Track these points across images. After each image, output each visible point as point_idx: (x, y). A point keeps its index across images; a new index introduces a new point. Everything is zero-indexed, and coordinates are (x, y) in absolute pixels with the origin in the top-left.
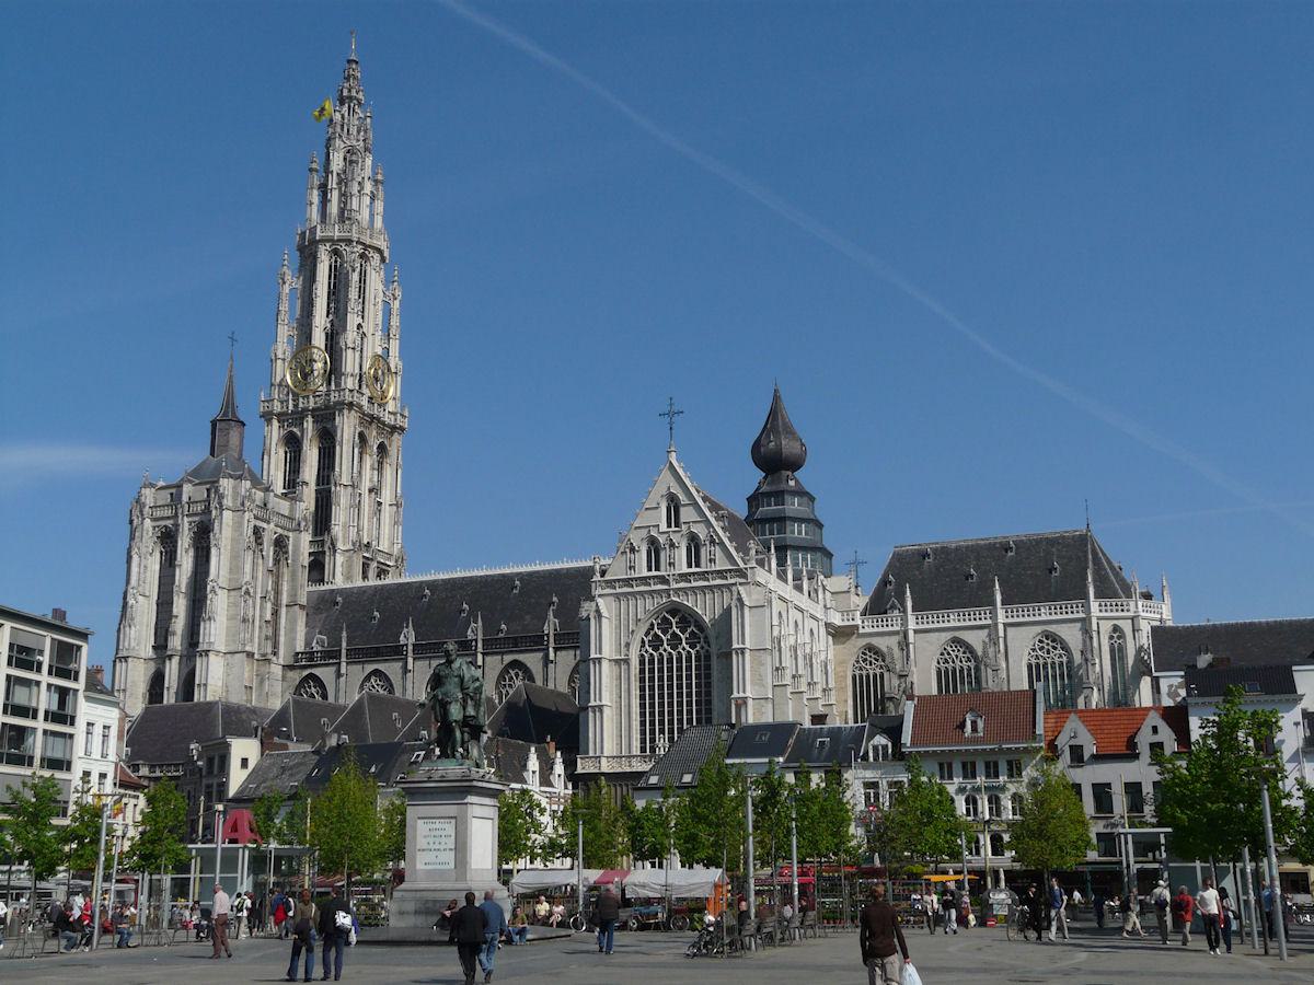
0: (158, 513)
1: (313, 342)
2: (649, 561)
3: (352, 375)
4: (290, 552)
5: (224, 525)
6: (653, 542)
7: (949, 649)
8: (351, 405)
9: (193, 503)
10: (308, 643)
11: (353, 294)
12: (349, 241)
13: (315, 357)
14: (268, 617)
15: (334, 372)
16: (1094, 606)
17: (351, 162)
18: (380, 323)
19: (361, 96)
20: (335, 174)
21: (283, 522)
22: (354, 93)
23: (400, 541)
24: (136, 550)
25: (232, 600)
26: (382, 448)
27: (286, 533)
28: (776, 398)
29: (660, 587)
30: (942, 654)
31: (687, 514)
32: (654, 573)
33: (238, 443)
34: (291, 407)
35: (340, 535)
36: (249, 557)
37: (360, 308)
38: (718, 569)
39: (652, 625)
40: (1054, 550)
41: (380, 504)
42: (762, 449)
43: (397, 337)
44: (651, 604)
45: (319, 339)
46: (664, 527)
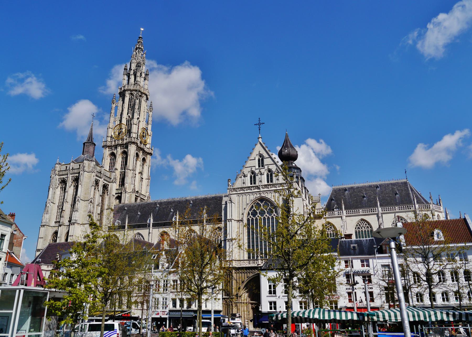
0: (61, 173)
1: (122, 122)
2: (251, 181)
3: (135, 133)
4: (109, 190)
5: (84, 177)
6: (253, 172)
7: (360, 223)
8: (134, 143)
9: (74, 169)
10: (114, 224)
11: (137, 107)
12: (136, 90)
13: (123, 127)
14: (99, 212)
15: (129, 132)
16: (417, 206)
17: (138, 66)
18: (145, 118)
19: (142, 47)
20: (133, 70)
21: (106, 179)
22: (140, 46)
24: (52, 186)
25: (85, 205)
26: (144, 160)
27: (108, 183)
28: (287, 136)
29: (256, 190)
30: (357, 225)
31: (267, 161)
32: (253, 185)
33: (92, 151)
35: (128, 187)
36: (93, 187)
37: (139, 112)
38: (280, 182)
39: (253, 206)
40: (395, 187)
41: (142, 178)
42: (283, 153)
43: (151, 124)
44: (252, 197)
45: (124, 121)
46: (257, 167)
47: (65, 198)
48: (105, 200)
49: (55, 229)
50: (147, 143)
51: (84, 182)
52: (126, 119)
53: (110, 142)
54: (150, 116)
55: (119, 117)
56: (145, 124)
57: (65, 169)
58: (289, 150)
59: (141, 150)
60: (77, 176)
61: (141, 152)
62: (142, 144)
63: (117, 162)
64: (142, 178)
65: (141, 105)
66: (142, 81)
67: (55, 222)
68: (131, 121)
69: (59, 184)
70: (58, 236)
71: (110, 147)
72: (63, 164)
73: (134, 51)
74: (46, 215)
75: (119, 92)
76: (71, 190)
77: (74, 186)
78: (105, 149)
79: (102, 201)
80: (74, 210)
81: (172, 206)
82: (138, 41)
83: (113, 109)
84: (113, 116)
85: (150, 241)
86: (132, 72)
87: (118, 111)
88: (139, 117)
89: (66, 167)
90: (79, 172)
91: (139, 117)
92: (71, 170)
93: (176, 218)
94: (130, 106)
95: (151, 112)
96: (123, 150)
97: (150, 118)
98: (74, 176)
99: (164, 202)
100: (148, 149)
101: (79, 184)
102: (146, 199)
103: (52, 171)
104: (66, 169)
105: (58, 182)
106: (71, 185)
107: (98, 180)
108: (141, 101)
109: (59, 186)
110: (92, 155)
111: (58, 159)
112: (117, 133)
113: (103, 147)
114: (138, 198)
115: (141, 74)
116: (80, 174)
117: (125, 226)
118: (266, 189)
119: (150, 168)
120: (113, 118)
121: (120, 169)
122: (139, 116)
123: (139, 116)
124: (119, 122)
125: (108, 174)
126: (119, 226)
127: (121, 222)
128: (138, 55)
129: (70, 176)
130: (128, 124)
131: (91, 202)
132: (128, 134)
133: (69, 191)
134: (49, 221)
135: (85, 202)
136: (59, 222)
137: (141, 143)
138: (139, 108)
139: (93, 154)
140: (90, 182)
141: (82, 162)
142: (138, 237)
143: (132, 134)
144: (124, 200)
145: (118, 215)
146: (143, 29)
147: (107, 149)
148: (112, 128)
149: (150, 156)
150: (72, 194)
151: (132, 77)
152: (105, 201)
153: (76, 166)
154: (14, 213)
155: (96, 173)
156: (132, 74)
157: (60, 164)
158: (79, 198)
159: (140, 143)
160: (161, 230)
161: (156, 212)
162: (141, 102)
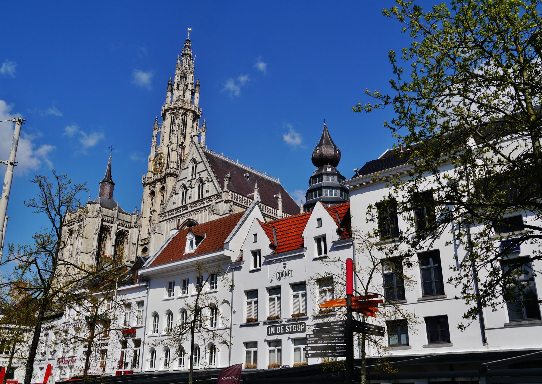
27: (126, 229)
52: (168, 146)
54: (203, 138)
58: (322, 149)
65: (186, 125)
71: (149, 184)
88: (183, 140)
91: (183, 140)
95: (203, 132)
107: (109, 226)
108: (186, 120)
118: (195, 208)
122: (185, 139)
138: (183, 129)
146: (191, 29)
156: (176, 88)
162: (186, 121)
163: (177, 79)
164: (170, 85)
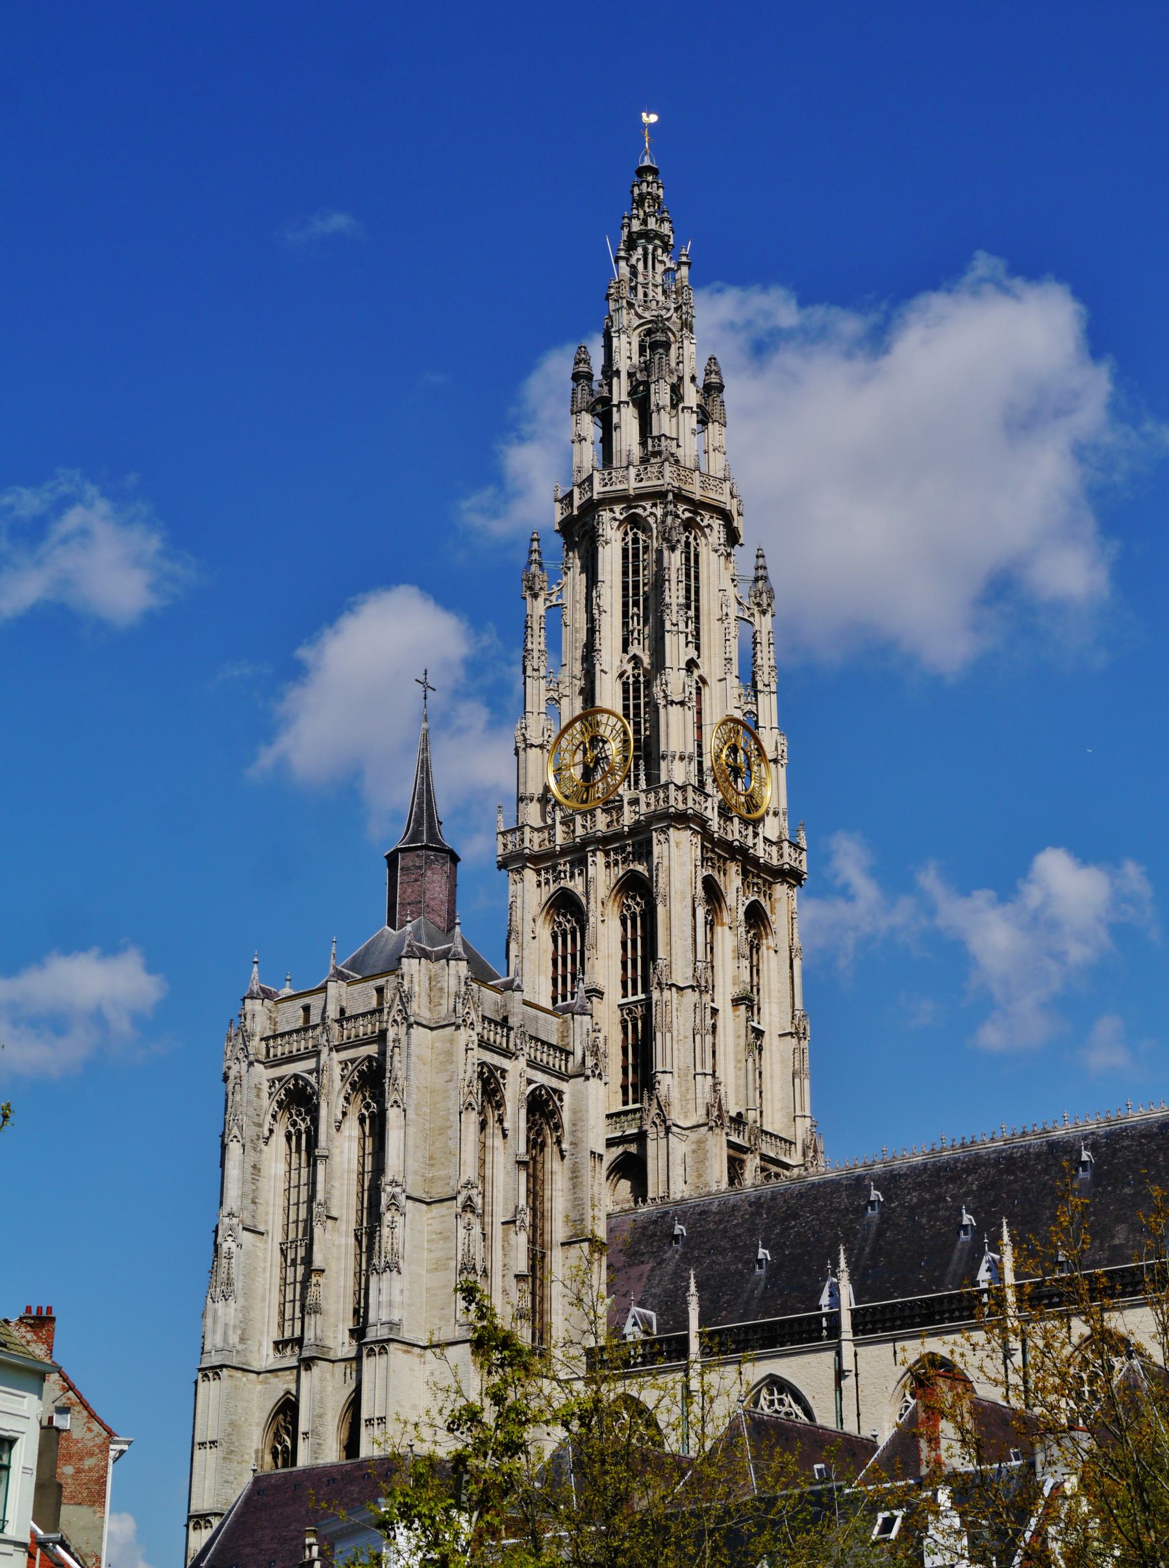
0: (281, 1048)
1: (598, 703)
3: (682, 758)
5: (413, 1059)
8: (682, 819)
9: (348, 1019)
11: (674, 595)
12: (658, 496)
13: (605, 731)
14: (522, 1266)
17: (654, 346)
18: (735, 656)
19: (666, 228)
20: (624, 375)
21: (543, 1057)
22: (652, 224)
23: (808, 1113)
24: (235, 1131)
26: (756, 917)
27: (554, 1083)
34: (559, 839)
35: (675, 1095)
36: (473, 1118)
37: (691, 626)
41: (759, 1034)
43: (773, 688)
45: (609, 694)
47: (320, 1196)
48: (547, 1187)
49: (282, 1385)
50: (762, 811)
51: (413, 1089)
52: (621, 676)
53: (539, 830)
55: (578, 669)
56: (736, 692)
57: (300, 1023)
59: (733, 859)
60: (369, 1058)
61: (733, 868)
62: (731, 819)
63: (594, 946)
64: (754, 1029)
65: (697, 578)
66: (688, 431)
67: (276, 1344)
68: (648, 685)
69: (274, 1117)
70: (303, 1426)
71: (543, 861)
72: (287, 991)
73: (617, 259)
74: (220, 1305)
75: (559, 518)
76: (346, 1145)
77: (362, 1120)
78: (517, 877)
79: (535, 1194)
80: (375, 1261)
81: (967, 1194)
82: (636, 191)
83: (536, 627)
84: (543, 672)
85: (850, 1427)
86: (621, 389)
87: (566, 633)
88: (692, 653)
89: (306, 1009)
90: (383, 1034)
91: (694, 654)
92: (336, 1025)
93: (996, 1268)
94: (636, 594)
95: (764, 612)
96: (620, 871)
97: (765, 655)
98: (353, 1061)
99: (913, 1168)
100: (774, 849)
101: (388, 1105)
102: (795, 1159)
103: (230, 1039)
104: (307, 1018)
105: (268, 1105)
106: (344, 1114)
107: (497, 1068)
108: (697, 556)
109: (276, 1127)
110: (444, 925)
111: (255, 967)
112: (577, 772)
113: (502, 865)
114: (748, 1157)
115: (676, 390)
116: (390, 1044)
117: (686, 1339)
119: (797, 963)
120: (543, 682)
121: (620, 991)
122: (698, 648)
123: (698, 648)
124: (579, 702)
125: (550, 1028)
126: (652, 1343)
127: (660, 1315)
128: (645, 276)
129: (333, 1062)
130: (637, 707)
131: (468, 1206)
132: (642, 767)
133: (335, 1152)
134: (242, 1340)
135: (436, 1209)
136: (299, 1342)
137: (725, 812)
138: (688, 598)
139: (452, 913)
140: (451, 1085)
141: (393, 968)
142: (772, 1403)
143: (663, 764)
144: (663, 1177)
145: (634, 1272)
146: (653, 118)
147: (529, 875)
148: (542, 747)
149: (791, 886)
150: (355, 1166)
151: (627, 420)
152: (547, 1193)
153: (361, 997)
154: (49, 1309)
155: (479, 1029)
156: (624, 398)
157: (267, 995)
158: (398, 1190)
159: (720, 815)
160: (913, 1350)
161: (865, 1239)
162: (697, 562)
163: (625, 353)
164: (583, 382)
